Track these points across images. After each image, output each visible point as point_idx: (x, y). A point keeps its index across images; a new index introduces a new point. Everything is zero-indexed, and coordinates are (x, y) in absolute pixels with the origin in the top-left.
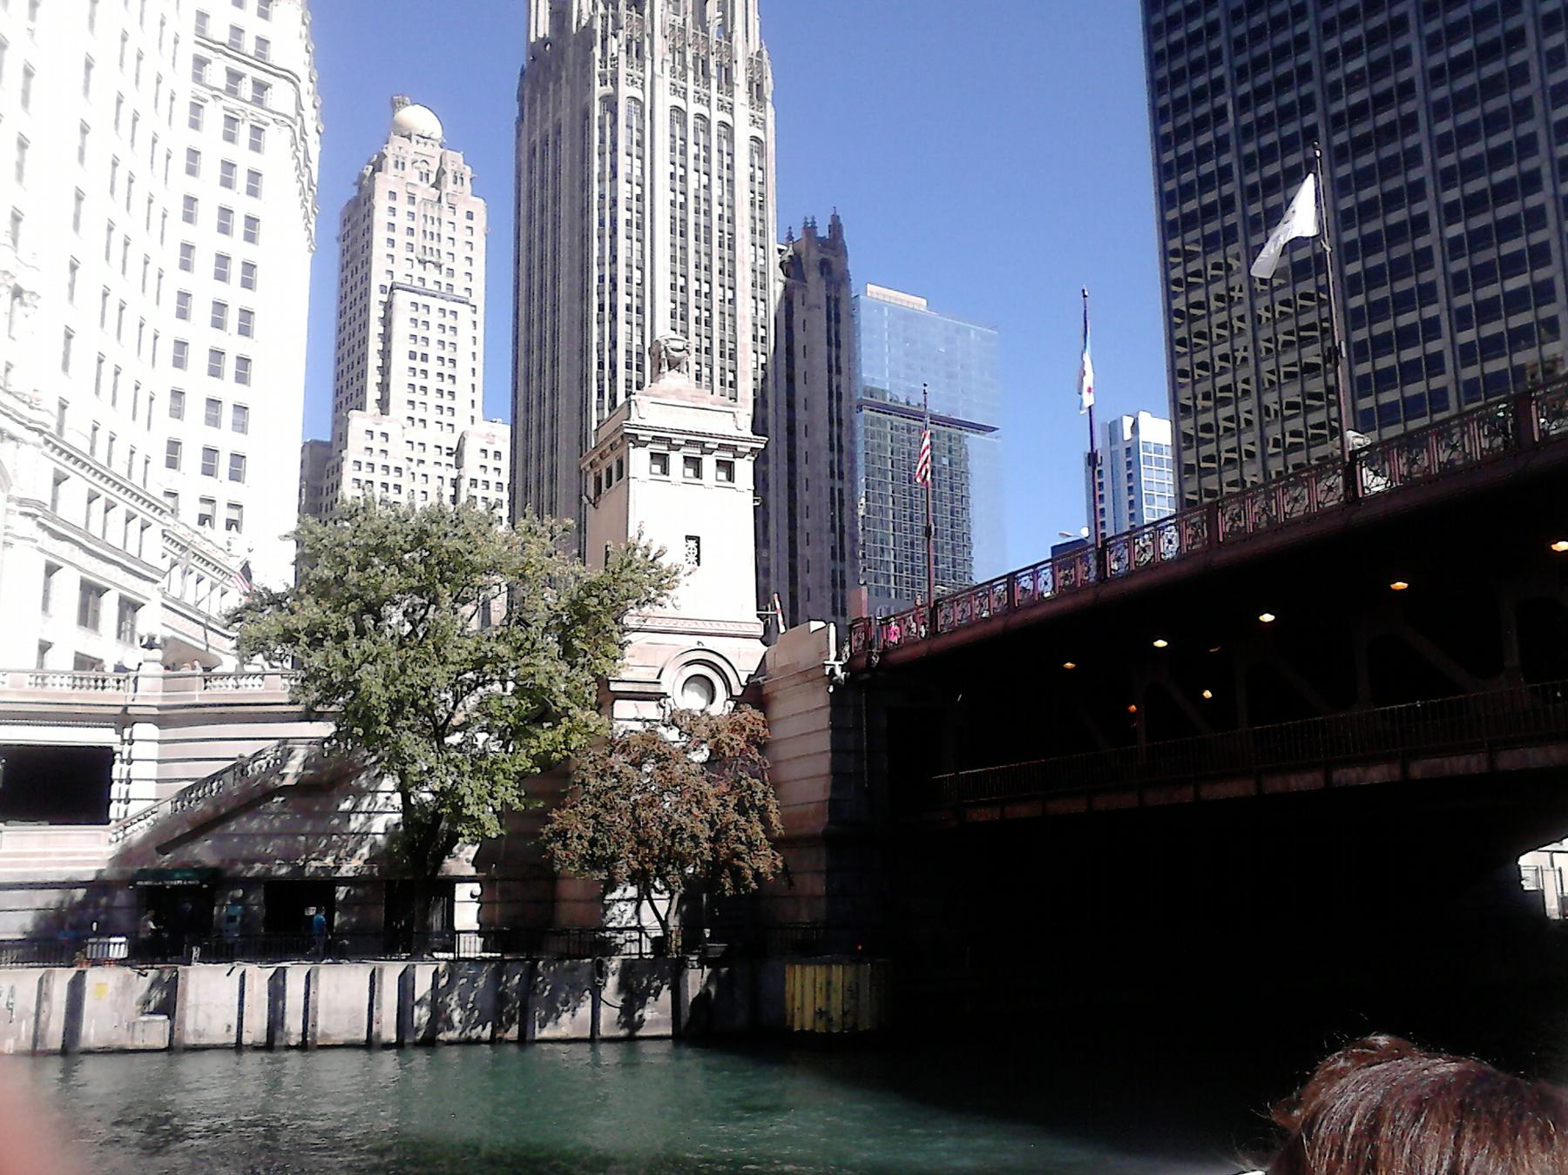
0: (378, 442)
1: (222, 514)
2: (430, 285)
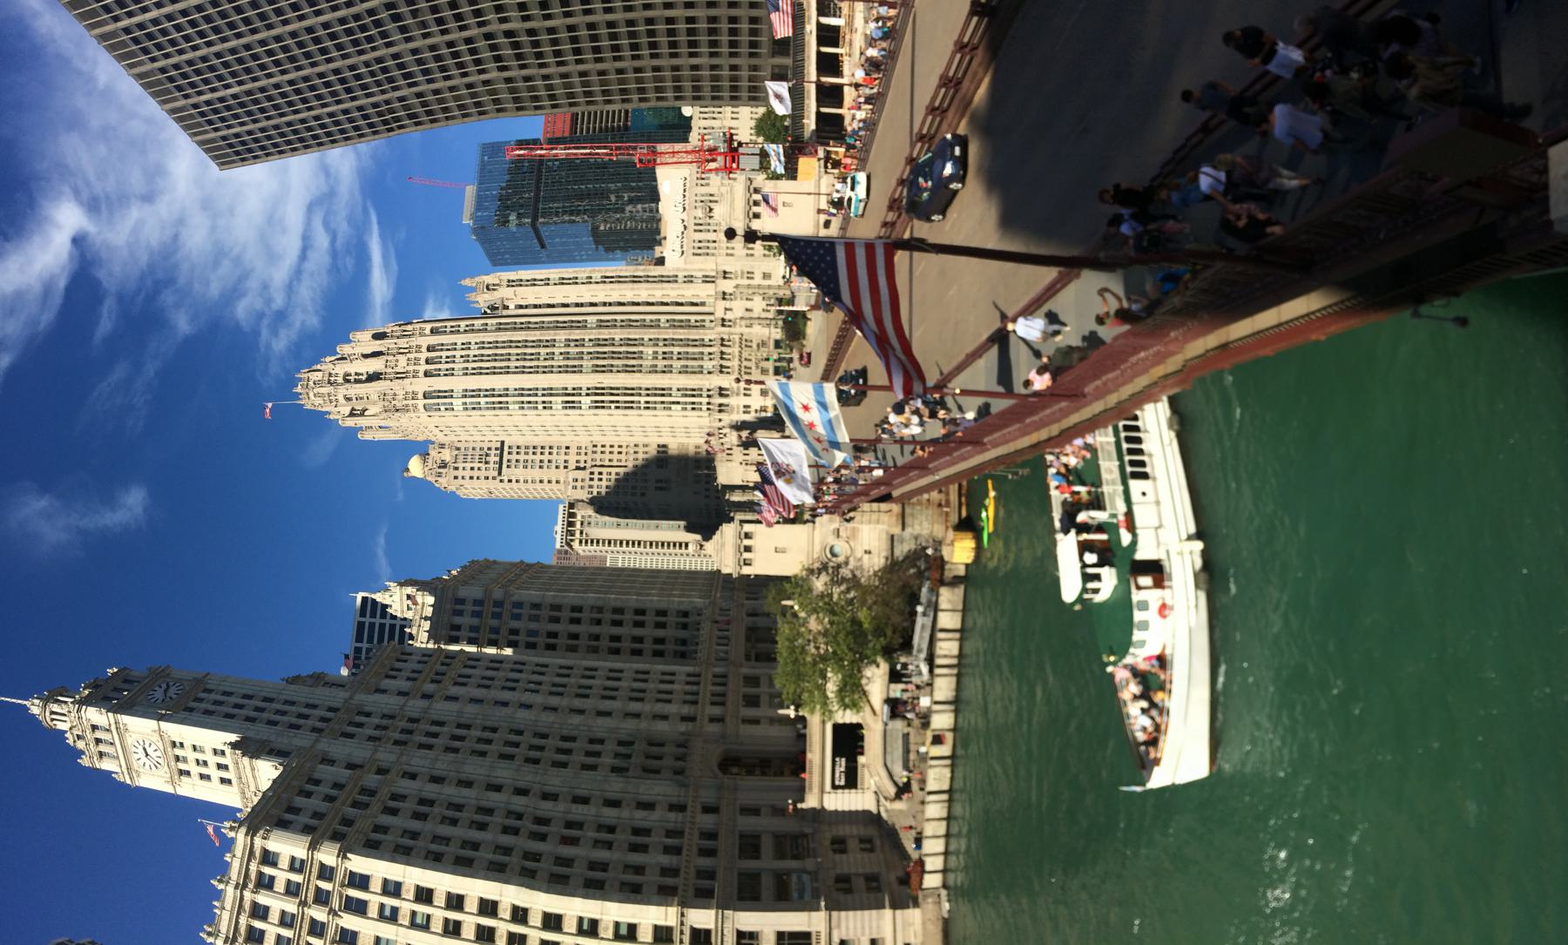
2: (497, 459)
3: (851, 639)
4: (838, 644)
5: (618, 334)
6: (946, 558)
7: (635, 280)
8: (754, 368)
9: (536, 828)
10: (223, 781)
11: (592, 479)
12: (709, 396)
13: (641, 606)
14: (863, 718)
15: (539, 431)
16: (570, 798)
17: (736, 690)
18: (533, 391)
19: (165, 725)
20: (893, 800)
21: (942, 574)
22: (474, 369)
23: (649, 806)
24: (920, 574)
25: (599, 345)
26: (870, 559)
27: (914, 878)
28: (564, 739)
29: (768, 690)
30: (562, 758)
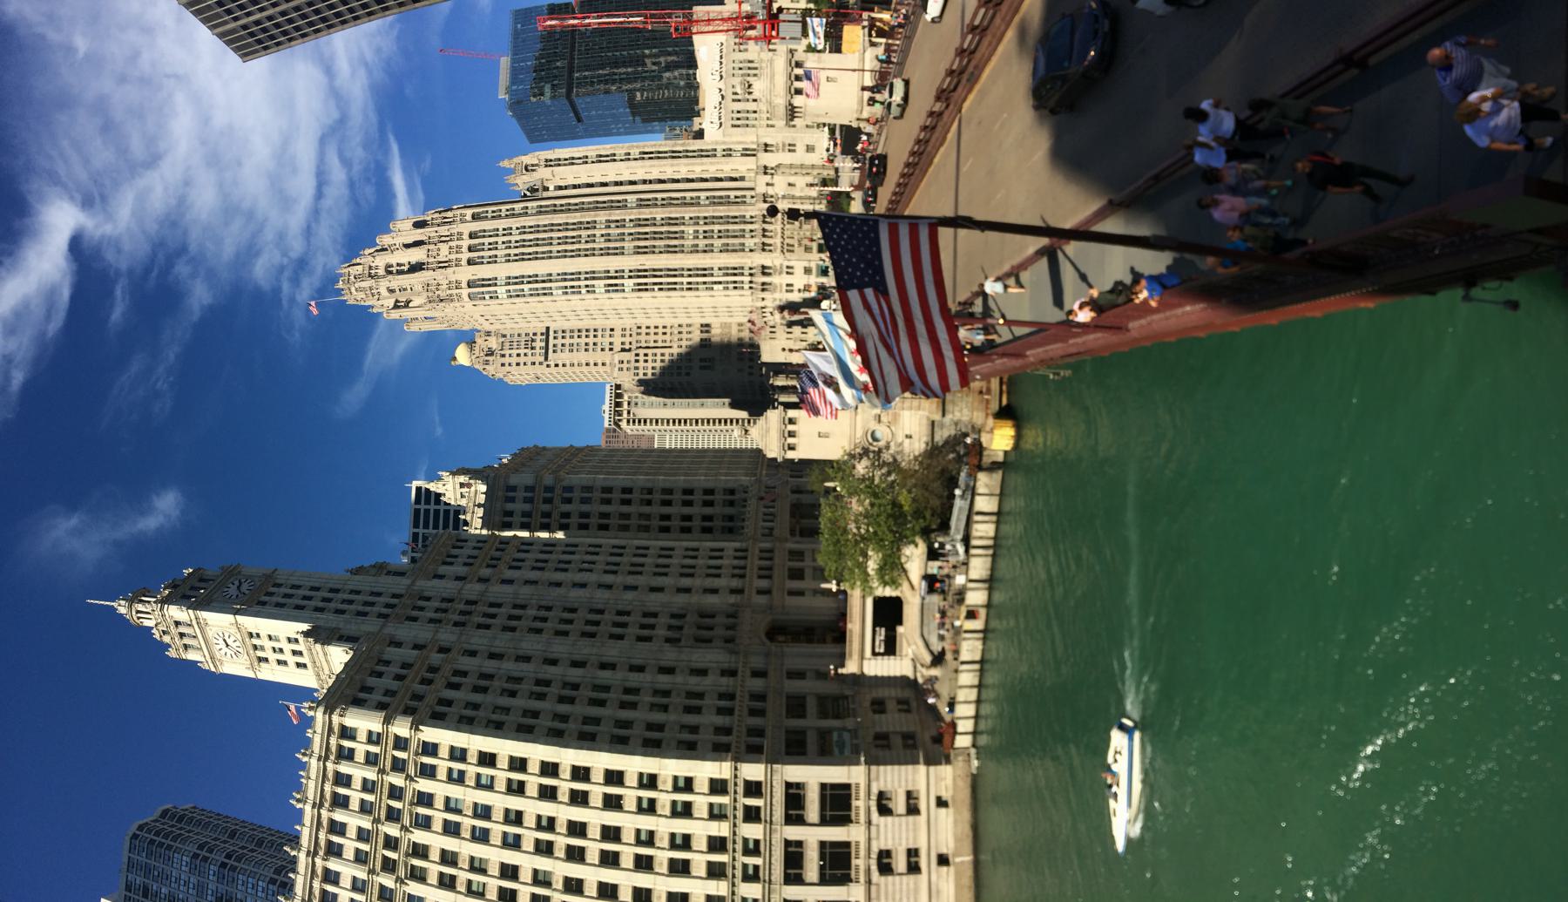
0: (625, 366)
2: (543, 344)
3: (891, 521)
4: (879, 525)
5: (659, 214)
6: (985, 445)
7: (675, 155)
8: (796, 245)
9: (595, 695)
10: (299, 665)
11: (637, 361)
12: (751, 275)
13: (687, 486)
14: (901, 592)
15: (583, 315)
16: (627, 667)
17: (781, 563)
18: (576, 276)
19: (241, 619)
20: (929, 667)
21: (980, 460)
22: (516, 255)
23: (702, 672)
24: (959, 459)
25: (640, 225)
26: (910, 443)
27: (947, 738)
28: (620, 613)
29: (812, 564)
30: (619, 631)
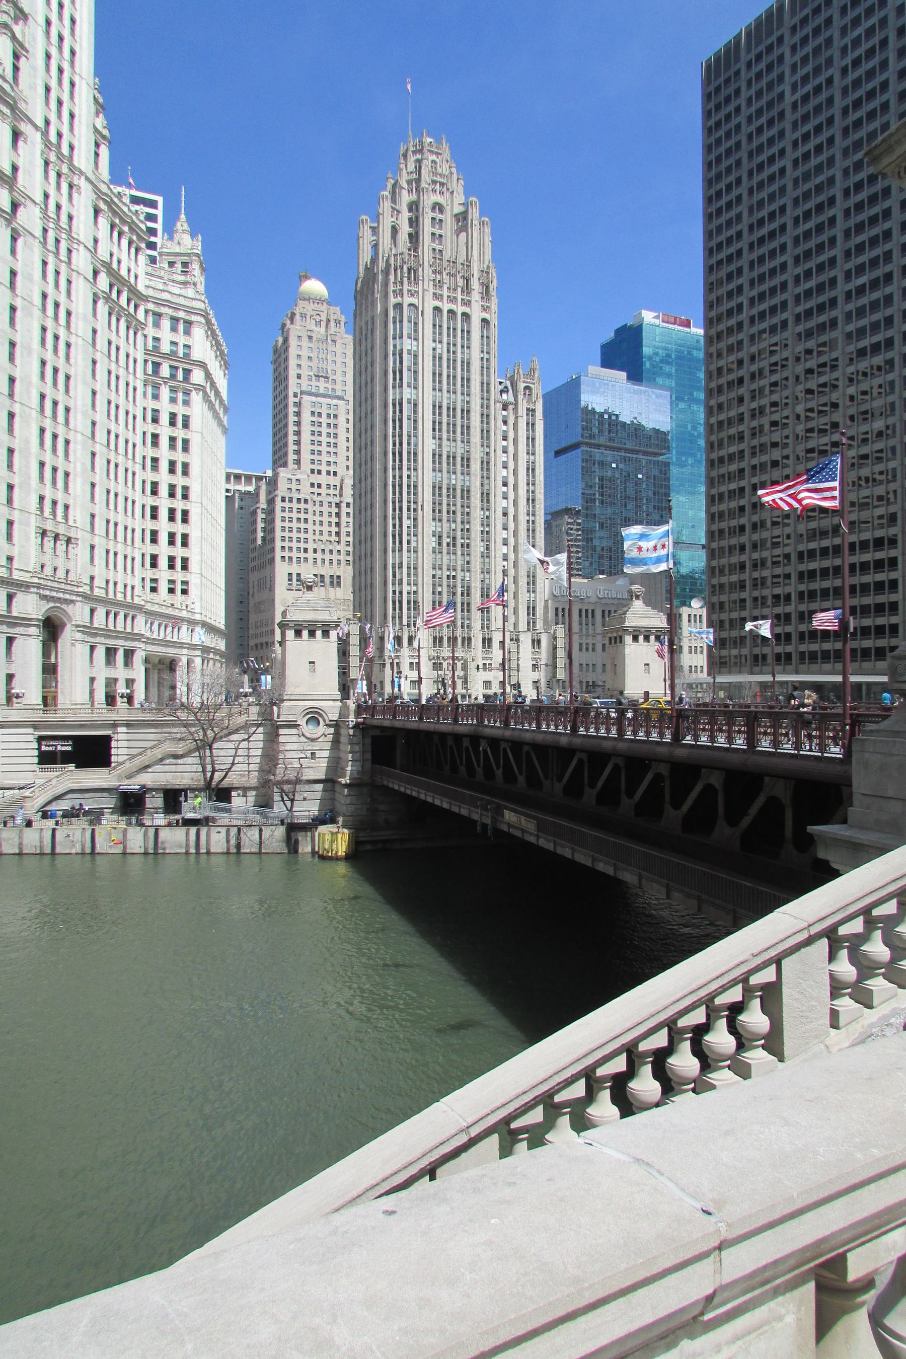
0: (294, 486)
1: (179, 587)
2: (322, 391)
11: (299, 500)
